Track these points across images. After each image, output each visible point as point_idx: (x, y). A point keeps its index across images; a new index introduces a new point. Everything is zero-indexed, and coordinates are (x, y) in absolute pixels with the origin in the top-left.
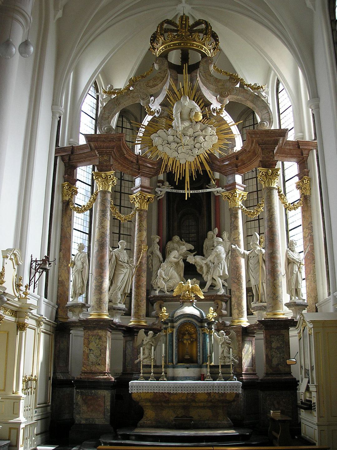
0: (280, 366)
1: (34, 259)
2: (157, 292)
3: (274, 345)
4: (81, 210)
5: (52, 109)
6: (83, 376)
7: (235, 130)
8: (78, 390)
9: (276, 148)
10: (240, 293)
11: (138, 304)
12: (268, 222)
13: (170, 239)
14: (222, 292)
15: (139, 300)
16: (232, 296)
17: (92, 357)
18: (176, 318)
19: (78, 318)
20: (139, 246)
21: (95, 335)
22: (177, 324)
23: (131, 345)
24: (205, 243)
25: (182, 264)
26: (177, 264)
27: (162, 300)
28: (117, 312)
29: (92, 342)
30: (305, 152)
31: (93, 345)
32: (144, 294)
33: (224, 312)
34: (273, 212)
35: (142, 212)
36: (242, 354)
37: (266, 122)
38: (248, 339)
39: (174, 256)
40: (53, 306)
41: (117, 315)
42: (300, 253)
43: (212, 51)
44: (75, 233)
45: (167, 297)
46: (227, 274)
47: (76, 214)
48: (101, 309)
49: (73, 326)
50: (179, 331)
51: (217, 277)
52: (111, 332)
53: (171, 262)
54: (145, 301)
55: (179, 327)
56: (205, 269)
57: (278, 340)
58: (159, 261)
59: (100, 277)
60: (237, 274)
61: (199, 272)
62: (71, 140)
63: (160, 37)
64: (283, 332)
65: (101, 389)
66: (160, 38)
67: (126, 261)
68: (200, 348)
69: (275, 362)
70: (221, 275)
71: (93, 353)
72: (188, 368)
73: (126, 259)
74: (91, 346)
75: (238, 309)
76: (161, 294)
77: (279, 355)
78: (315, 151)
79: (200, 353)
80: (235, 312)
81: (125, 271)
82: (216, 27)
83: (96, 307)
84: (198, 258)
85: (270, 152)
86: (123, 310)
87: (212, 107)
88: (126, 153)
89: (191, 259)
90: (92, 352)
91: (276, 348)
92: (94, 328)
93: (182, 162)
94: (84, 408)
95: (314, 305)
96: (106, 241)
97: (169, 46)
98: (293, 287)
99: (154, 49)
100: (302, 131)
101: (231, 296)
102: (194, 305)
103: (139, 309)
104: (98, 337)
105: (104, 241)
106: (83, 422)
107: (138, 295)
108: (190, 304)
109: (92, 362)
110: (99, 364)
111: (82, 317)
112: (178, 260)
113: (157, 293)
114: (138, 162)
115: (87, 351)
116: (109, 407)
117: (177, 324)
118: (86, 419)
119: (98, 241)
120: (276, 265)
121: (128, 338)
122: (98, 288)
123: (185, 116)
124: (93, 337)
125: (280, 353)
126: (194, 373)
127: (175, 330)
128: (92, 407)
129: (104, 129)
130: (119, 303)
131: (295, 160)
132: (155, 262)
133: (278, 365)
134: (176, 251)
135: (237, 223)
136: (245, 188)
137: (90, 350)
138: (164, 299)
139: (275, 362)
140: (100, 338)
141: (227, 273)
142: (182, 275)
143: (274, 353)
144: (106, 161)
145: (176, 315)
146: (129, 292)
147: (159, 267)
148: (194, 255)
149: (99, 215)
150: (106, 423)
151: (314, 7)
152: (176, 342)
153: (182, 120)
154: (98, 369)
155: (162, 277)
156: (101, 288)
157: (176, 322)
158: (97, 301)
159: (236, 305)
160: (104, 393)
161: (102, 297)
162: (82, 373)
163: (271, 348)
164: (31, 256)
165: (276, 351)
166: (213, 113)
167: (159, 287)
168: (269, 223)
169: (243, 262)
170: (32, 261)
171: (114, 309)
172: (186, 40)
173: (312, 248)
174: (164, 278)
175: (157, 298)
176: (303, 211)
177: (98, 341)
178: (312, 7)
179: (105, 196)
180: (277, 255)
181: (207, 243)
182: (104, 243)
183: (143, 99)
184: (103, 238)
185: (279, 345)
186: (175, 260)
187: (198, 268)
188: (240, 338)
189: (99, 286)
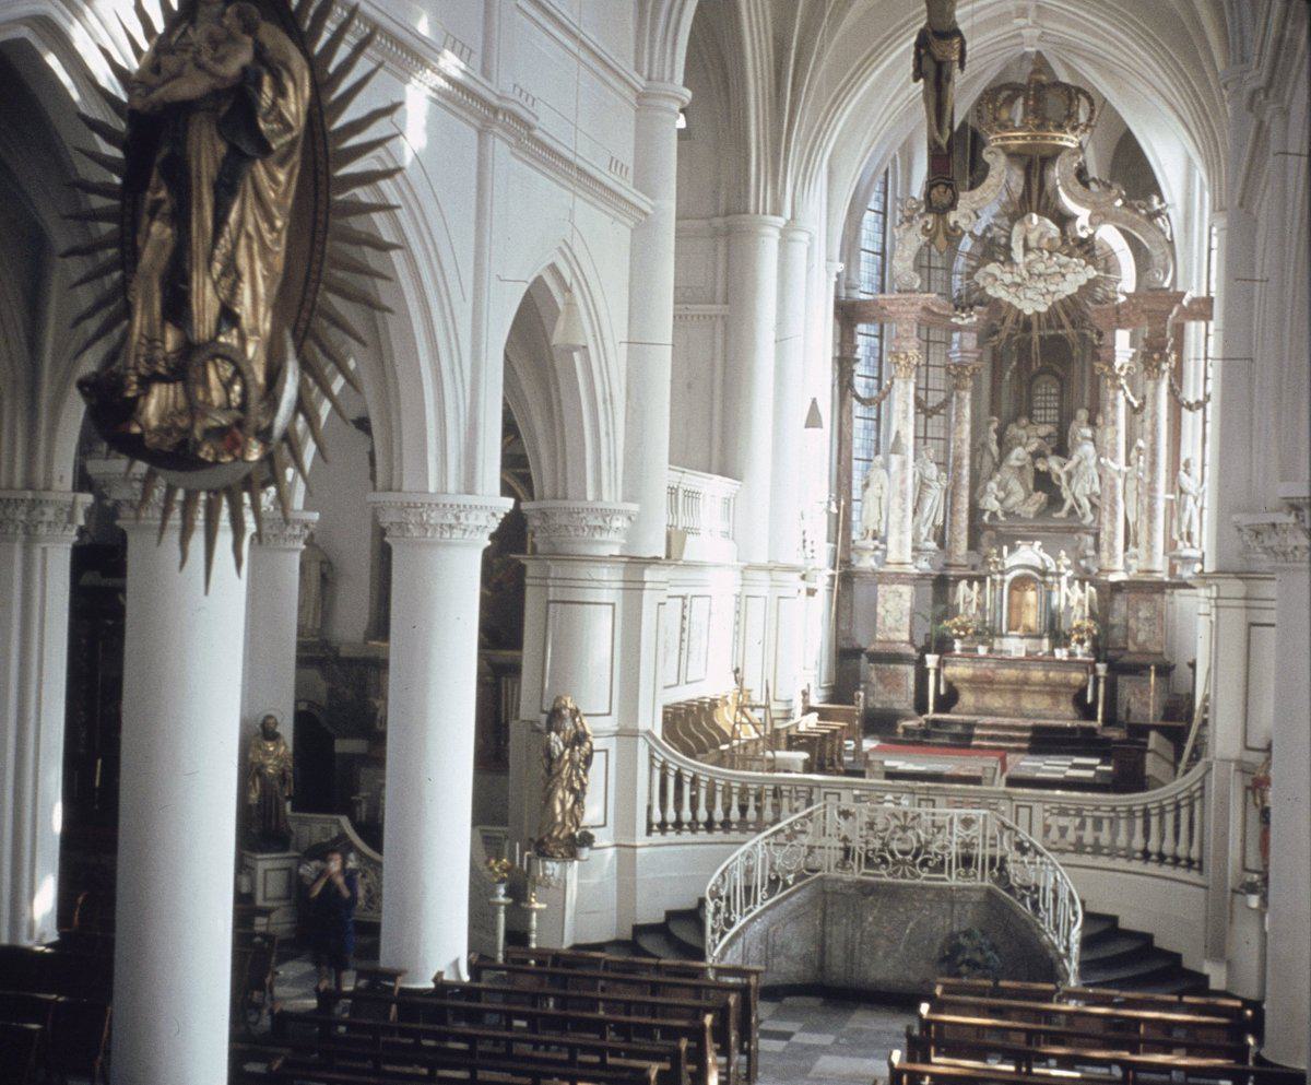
2: (986, 518)
13: (1015, 419)
17: (890, 622)
25: (1030, 468)
26: (1021, 468)
32: (963, 519)
33: (1091, 553)
35: (963, 393)
39: (1018, 455)
53: (1011, 467)
54: (965, 533)
64: (1156, 596)
67: (934, 477)
74: (888, 606)
80: (1104, 555)
93: (1028, 312)
94: (880, 687)
98: (1184, 530)
106: (878, 706)
117: (1008, 578)
118: (882, 702)
123: (1032, 244)
127: (1006, 586)
130: (926, 540)
132: (987, 461)
133: (1145, 642)
139: (1141, 637)
140: (900, 596)
141: (1096, 488)
142: (1031, 486)
145: (1007, 566)
147: (991, 478)
153: (1027, 249)
169: (1120, 482)
181: (1074, 426)
186: (1019, 463)
187: (1054, 477)
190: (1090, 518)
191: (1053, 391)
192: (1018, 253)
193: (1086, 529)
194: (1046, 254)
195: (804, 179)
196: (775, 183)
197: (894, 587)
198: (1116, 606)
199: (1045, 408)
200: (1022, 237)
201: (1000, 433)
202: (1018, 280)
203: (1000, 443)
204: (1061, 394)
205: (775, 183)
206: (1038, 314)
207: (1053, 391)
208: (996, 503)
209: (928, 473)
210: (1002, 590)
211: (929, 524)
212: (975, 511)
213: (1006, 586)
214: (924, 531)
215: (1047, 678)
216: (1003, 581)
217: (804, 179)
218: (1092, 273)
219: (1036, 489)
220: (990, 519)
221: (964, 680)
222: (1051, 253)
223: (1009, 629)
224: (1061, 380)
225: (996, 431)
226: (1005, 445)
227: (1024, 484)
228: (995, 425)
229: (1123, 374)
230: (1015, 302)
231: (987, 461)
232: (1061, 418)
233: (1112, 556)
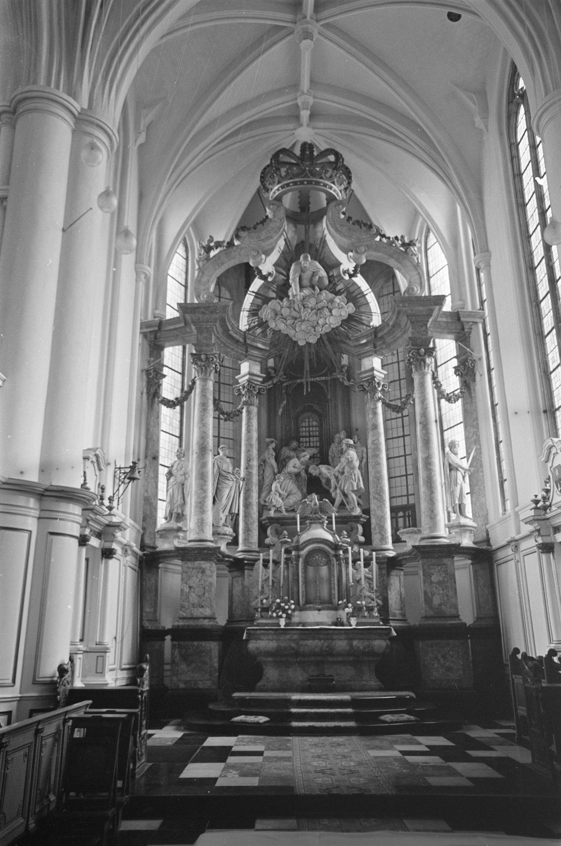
0: (443, 607)
1: (118, 466)
3: (434, 578)
4: (170, 404)
5: (136, 268)
6: (181, 623)
7: (371, 298)
8: (174, 643)
9: (430, 320)
10: (383, 512)
11: (248, 528)
12: (421, 417)
14: (358, 511)
15: (249, 523)
16: (372, 516)
18: (302, 544)
19: (172, 546)
20: (248, 451)
21: (196, 568)
22: (304, 552)
23: (240, 582)
24: (331, 449)
25: (303, 474)
26: (298, 475)
27: (279, 523)
28: (222, 538)
29: (193, 576)
30: (466, 327)
31: (194, 581)
33: (362, 539)
34: (427, 404)
35: (251, 407)
36: (387, 593)
37: (417, 287)
38: (394, 573)
40: (139, 531)
41: (222, 541)
42: (462, 458)
43: (343, 192)
44: (163, 436)
45: (284, 518)
46: (363, 487)
47: (164, 410)
48: (204, 532)
49: (164, 557)
50: (307, 563)
51: (351, 492)
52: (216, 564)
53: (290, 473)
55: (306, 556)
56: (333, 481)
57: (439, 572)
58: (272, 474)
59: (201, 491)
60: (377, 487)
61: (325, 486)
62: (157, 312)
63: (276, 173)
64: (446, 561)
65: (206, 640)
66: (275, 175)
68: (334, 583)
69: (436, 601)
70: (355, 489)
71: (194, 592)
72: (319, 610)
73: (230, 469)
74: (191, 583)
75: (380, 533)
76: (278, 515)
77: (441, 592)
78: (480, 326)
79: (334, 589)
80: (376, 538)
81: (231, 483)
82: (349, 160)
83: (198, 531)
84: (324, 469)
85: (422, 326)
86: (231, 536)
87: (342, 267)
88: (230, 328)
89: (314, 471)
90: (192, 590)
91: (437, 583)
92: (196, 560)
95: (484, 527)
96: (208, 443)
97: (288, 185)
99: (267, 190)
100: (462, 298)
101: (370, 518)
102: (325, 527)
103: (249, 534)
104: (201, 570)
105: (206, 443)
107: (247, 515)
108: (319, 525)
109: (193, 604)
110: (202, 607)
111: (177, 543)
112: (299, 471)
113: (272, 513)
114: (245, 341)
115: (187, 590)
116: (216, 665)
117: (304, 552)
119: (198, 443)
120: (433, 474)
121: (235, 574)
122: (199, 505)
124: (195, 570)
125: (443, 590)
126: (328, 617)
128: (193, 665)
129: (203, 297)
130: (224, 525)
131: (452, 336)
132: (268, 473)
133: (440, 605)
134: (296, 459)
135: (376, 420)
136: (385, 375)
137: (190, 587)
138: (281, 521)
140: (203, 572)
141: (362, 485)
143: (434, 589)
144: (206, 338)
146: (237, 512)
148: (317, 465)
149: (198, 409)
150: (213, 687)
151: (486, 126)
152: (302, 577)
154: (201, 613)
155: (278, 492)
156: (203, 505)
157: (302, 549)
158: (198, 522)
159: (377, 529)
160: (209, 645)
161: (205, 517)
162: (180, 618)
163: (431, 583)
164: (115, 462)
165: (438, 586)
166: (343, 275)
167: (274, 506)
168: (423, 419)
170: (116, 468)
171: (219, 534)
172: (309, 177)
173: (479, 452)
174: (280, 495)
175: (272, 520)
176: (464, 405)
177: (200, 575)
178: (482, 127)
179: (206, 385)
180: (433, 460)
181: (333, 448)
182: (206, 445)
183: (254, 257)
184: (205, 440)
185: (441, 579)
186: (296, 470)
187: (323, 481)
188: (384, 572)
189: (200, 503)
190: (358, 511)
191: (315, 423)
192: (294, 290)
193: (356, 519)
194: (318, 290)
195: (105, 78)
196: (70, 70)
197: (197, 563)
198: (392, 581)
199: (310, 436)
200: (297, 275)
201: (277, 451)
202: (294, 314)
203: (276, 459)
204: (320, 426)
205: (70, 70)
206: (308, 344)
207: (315, 423)
208: (280, 500)
209: (225, 467)
210: (297, 565)
211: (227, 512)
212: (262, 508)
213: (301, 560)
214: (223, 516)
215: (351, 646)
216: (298, 557)
217: (105, 78)
218: (350, 308)
219: (309, 492)
220: (275, 511)
221: (268, 653)
222: (321, 290)
223: (307, 602)
224: (320, 416)
225: (274, 449)
226: (282, 463)
227: (299, 487)
228: (273, 445)
229: (380, 389)
230: (291, 333)
231: (268, 473)
232: (321, 441)
233: (383, 539)
